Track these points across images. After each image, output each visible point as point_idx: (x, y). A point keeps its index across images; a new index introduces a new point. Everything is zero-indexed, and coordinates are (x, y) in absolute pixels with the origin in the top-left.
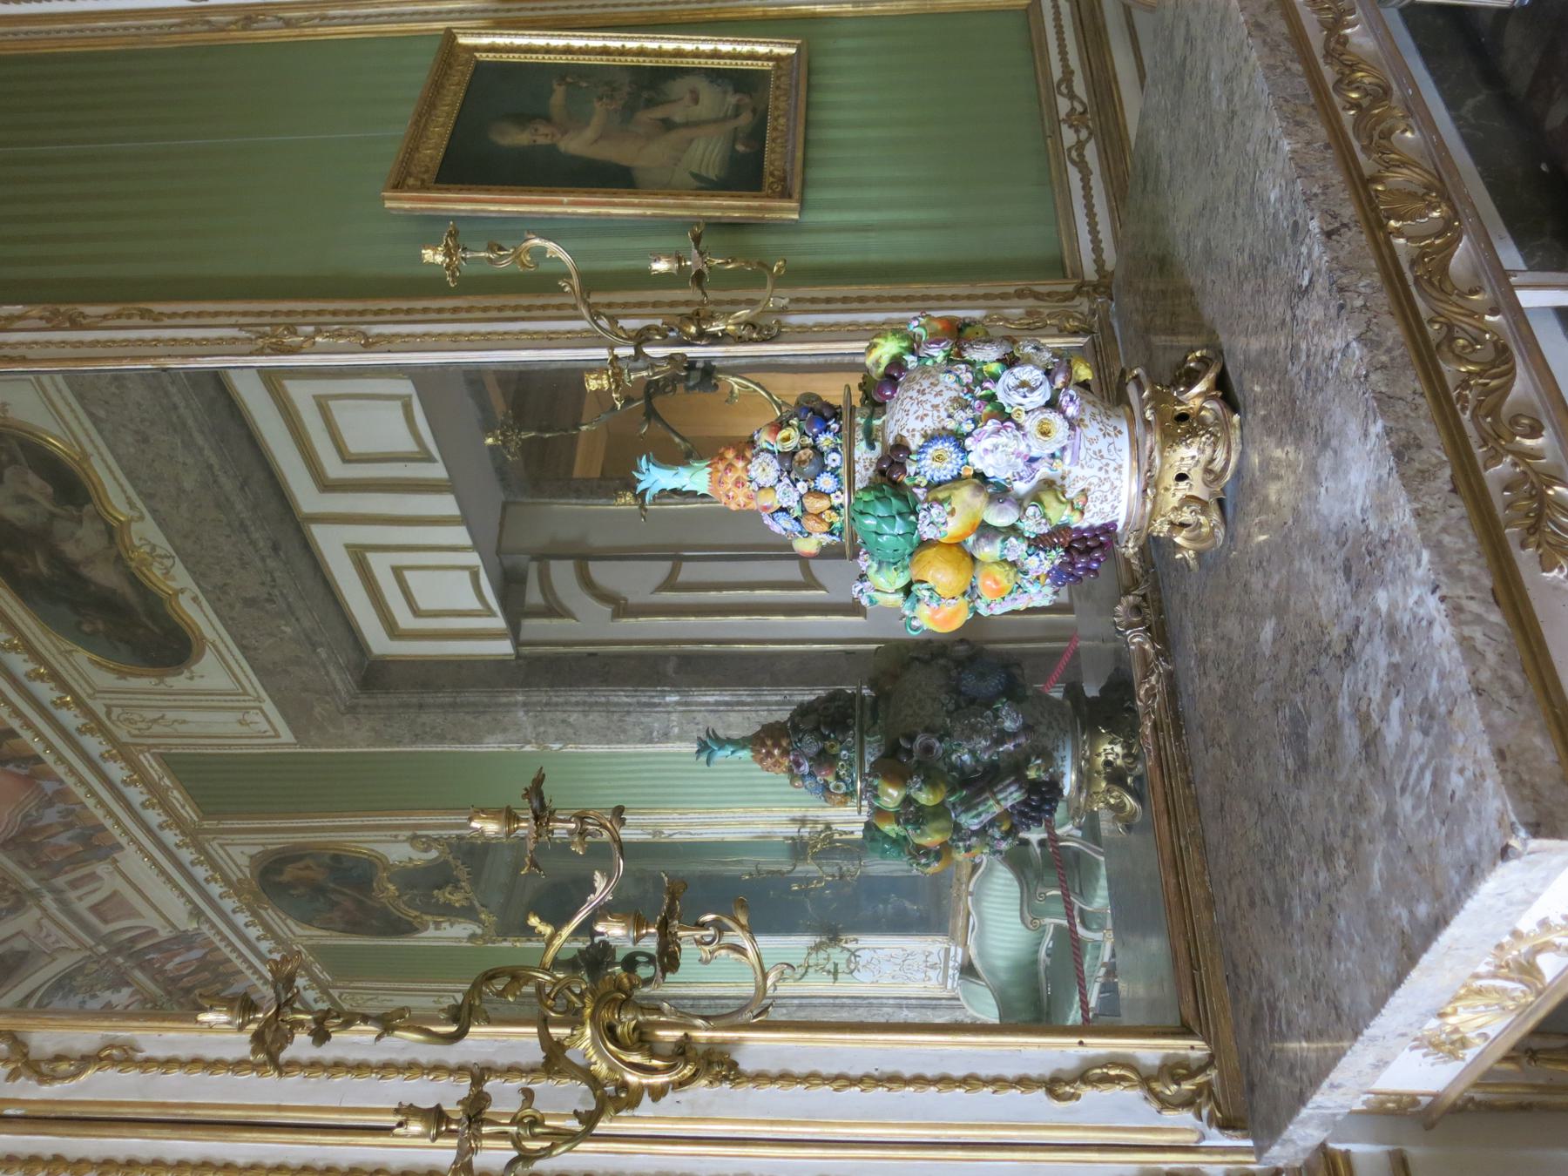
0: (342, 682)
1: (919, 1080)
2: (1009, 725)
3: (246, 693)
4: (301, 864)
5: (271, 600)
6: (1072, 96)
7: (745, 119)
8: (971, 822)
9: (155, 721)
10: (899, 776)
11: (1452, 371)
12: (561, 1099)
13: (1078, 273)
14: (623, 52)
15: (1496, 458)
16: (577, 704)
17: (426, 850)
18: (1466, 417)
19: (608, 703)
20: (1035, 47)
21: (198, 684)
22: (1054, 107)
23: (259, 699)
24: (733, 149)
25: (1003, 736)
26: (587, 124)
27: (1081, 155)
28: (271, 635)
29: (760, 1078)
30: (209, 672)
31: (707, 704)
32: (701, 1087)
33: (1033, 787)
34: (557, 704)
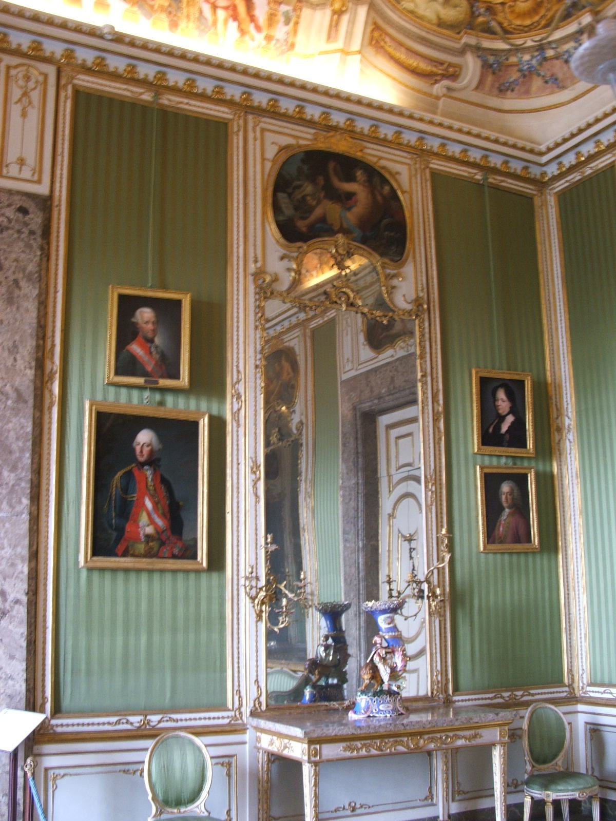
0: (366, 406)
1: (257, 656)
3: (359, 365)
5: (394, 388)
6: (522, 696)
11: (378, 742)
16: (358, 505)
17: (296, 428)
18: (369, 741)
19: (358, 518)
21: (361, 347)
22: (518, 690)
23: (357, 370)
28: (382, 384)
29: (257, 626)
30: (366, 352)
31: (358, 559)
32: (255, 615)
34: (358, 497)
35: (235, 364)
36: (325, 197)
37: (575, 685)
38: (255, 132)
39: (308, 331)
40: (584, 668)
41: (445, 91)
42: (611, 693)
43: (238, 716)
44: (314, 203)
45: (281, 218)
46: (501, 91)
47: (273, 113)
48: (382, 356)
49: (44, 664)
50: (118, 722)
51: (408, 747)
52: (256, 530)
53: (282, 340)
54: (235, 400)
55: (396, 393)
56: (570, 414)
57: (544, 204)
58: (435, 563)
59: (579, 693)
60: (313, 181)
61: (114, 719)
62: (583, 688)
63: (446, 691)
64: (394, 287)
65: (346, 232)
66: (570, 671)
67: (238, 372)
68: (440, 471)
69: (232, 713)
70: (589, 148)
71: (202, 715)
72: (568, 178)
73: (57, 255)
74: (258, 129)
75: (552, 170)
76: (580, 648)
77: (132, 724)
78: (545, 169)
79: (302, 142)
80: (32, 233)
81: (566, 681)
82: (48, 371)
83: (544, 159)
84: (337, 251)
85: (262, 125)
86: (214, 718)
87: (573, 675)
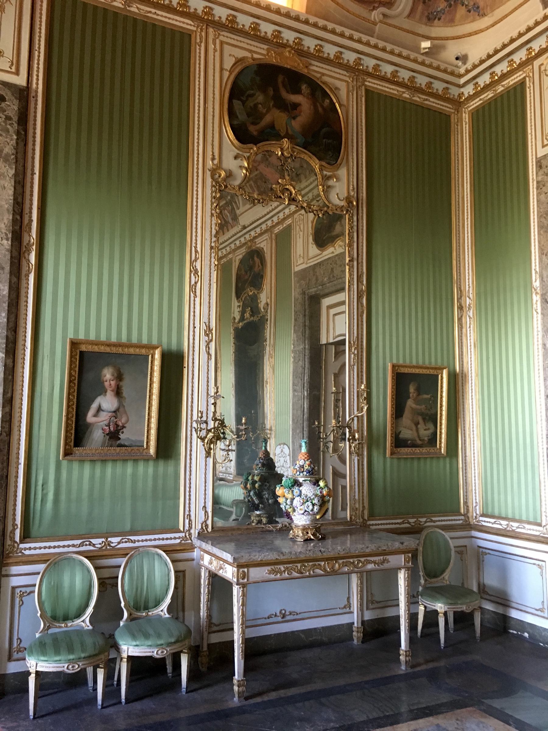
0: (313, 291)
1: (205, 486)
2: (270, 501)
3: (309, 260)
4: (260, 264)
5: (333, 277)
6: (426, 522)
7: (419, 442)
8: (252, 493)
9: (300, 228)
10: (260, 480)
12: (203, 433)
13: (369, 520)
14: (441, 410)
15: (284, 567)
16: (305, 364)
17: (264, 308)
19: (304, 373)
20: (445, 513)
21: (310, 245)
22: (422, 517)
23: (307, 264)
24: (408, 440)
25: (268, 500)
26: (417, 405)
27: (406, 523)
28: (324, 273)
29: (206, 461)
30: (313, 250)
32: (204, 452)
33: (258, 505)
34: (305, 358)
35: (194, 245)
36: (274, 106)
37: (470, 515)
38: (215, 44)
39: (273, 235)
40: (478, 501)
41: (381, 16)
42: (501, 525)
43: (188, 537)
44: (264, 111)
45: (235, 122)
46: (429, 19)
47: (231, 26)
48: (325, 253)
49: (16, 496)
51: (325, 570)
52: (208, 382)
53: (256, 242)
54: (192, 275)
55: (334, 281)
56: (471, 296)
57: (460, 120)
58: (356, 412)
59: (473, 522)
60: (264, 91)
61: (78, 542)
62: (476, 517)
63: (363, 517)
64: (329, 187)
65: (291, 138)
66: (466, 503)
67: (196, 251)
68: (362, 338)
69: (183, 534)
70: (503, 68)
71: (157, 536)
72: (482, 97)
73: (34, 141)
74: (218, 41)
75: (469, 90)
76: (474, 485)
77: (94, 545)
78: (462, 90)
79: (256, 56)
80: (8, 118)
81: (462, 511)
82: (25, 243)
83: (462, 81)
84: (282, 154)
85: (221, 38)
86: (167, 539)
87: (468, 506)
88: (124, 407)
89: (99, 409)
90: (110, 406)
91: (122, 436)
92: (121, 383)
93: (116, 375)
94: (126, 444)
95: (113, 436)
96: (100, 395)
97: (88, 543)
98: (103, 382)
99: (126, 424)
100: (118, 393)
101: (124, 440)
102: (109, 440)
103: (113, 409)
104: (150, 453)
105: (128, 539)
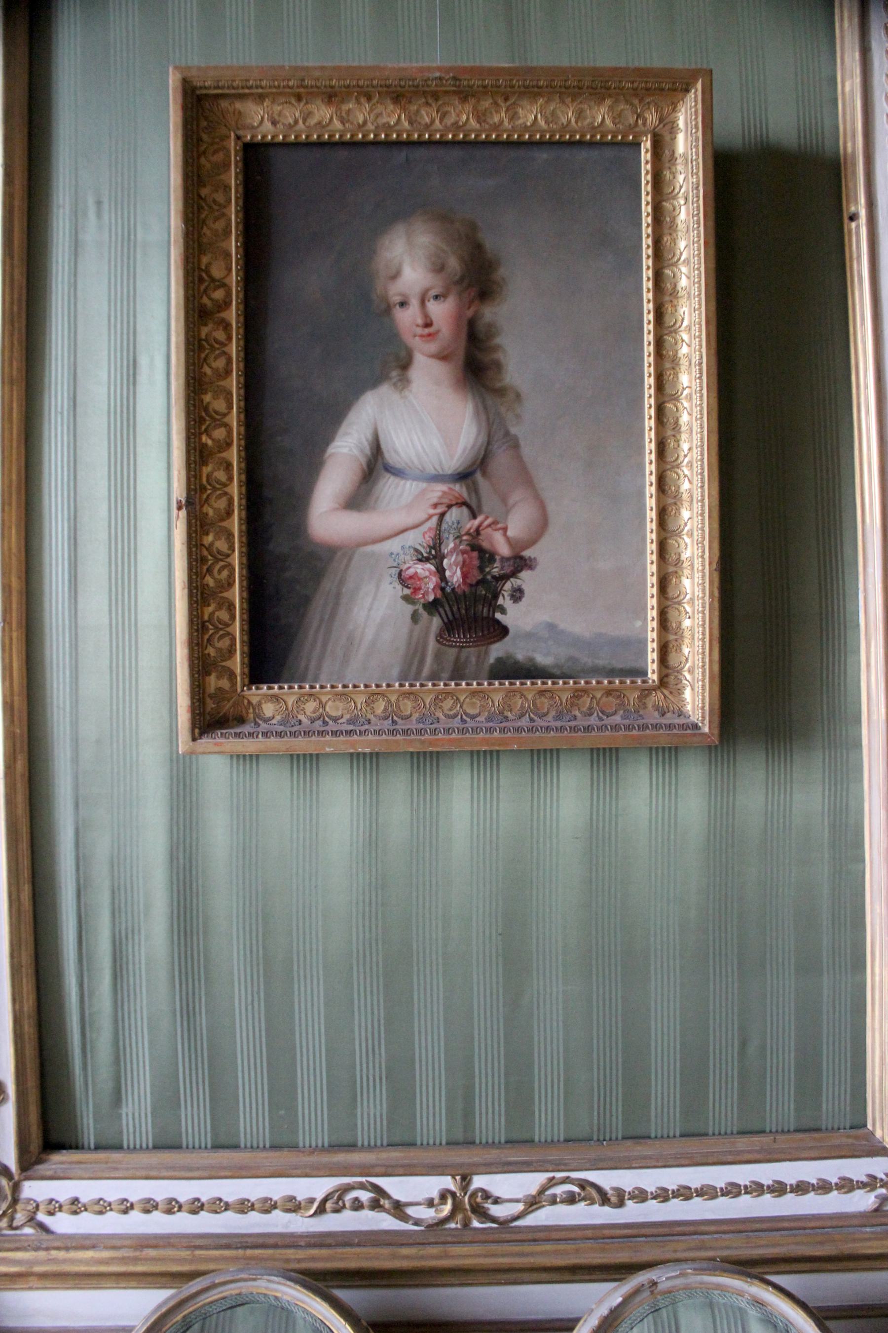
50: (333, 1202)
77: (398, 1209)
86: (801, 1188)
88: (515, 445)
89: (376, 465)
90: (437, 443)
91: (513, 615)
92: (488, 313)
93: (454, 264)
94: (543, 660)
95: (467, 612)
96: (375, 382)
97: (365, 1196)
98: (388, 310)
99: (532, 542)
100: (476, 365)
101: (529, 636)
102: (440, 638)
103: (454, 462)
104: (681, 714)
105: (583, 1184)
